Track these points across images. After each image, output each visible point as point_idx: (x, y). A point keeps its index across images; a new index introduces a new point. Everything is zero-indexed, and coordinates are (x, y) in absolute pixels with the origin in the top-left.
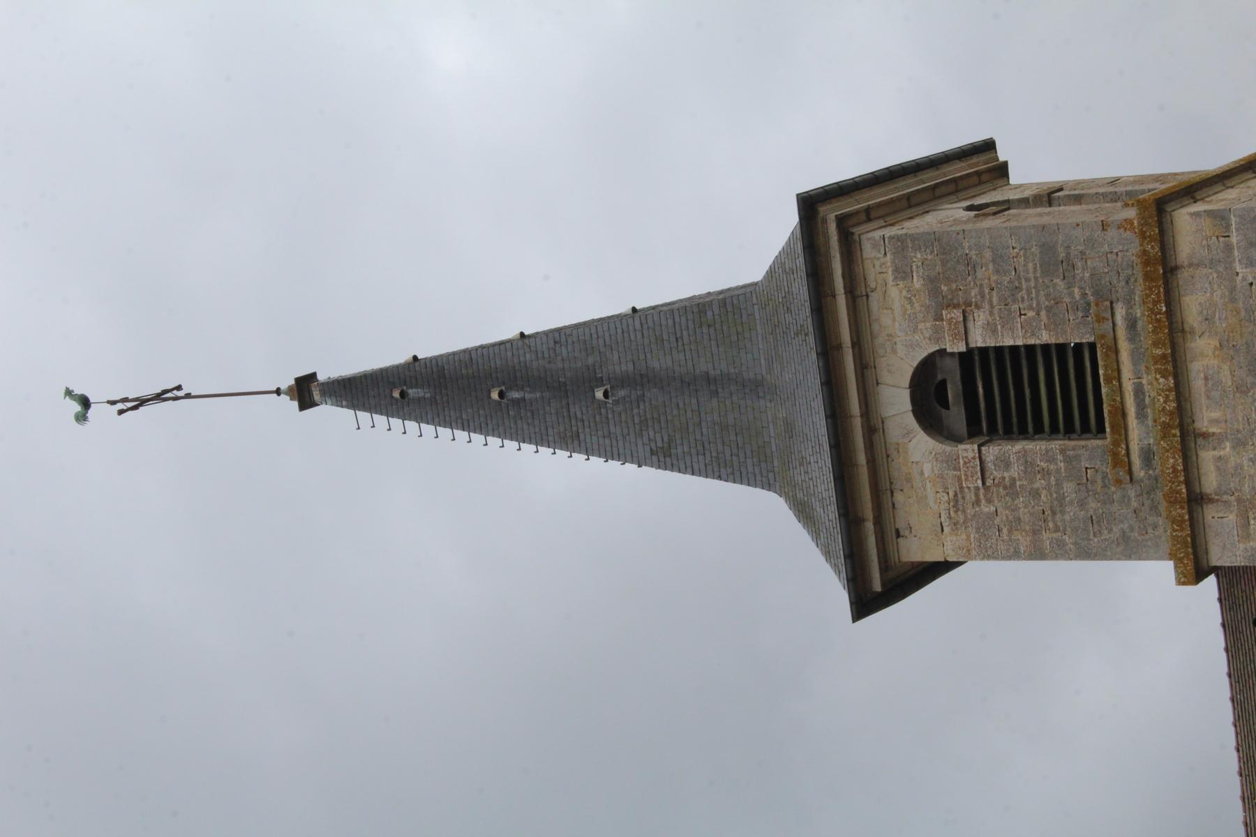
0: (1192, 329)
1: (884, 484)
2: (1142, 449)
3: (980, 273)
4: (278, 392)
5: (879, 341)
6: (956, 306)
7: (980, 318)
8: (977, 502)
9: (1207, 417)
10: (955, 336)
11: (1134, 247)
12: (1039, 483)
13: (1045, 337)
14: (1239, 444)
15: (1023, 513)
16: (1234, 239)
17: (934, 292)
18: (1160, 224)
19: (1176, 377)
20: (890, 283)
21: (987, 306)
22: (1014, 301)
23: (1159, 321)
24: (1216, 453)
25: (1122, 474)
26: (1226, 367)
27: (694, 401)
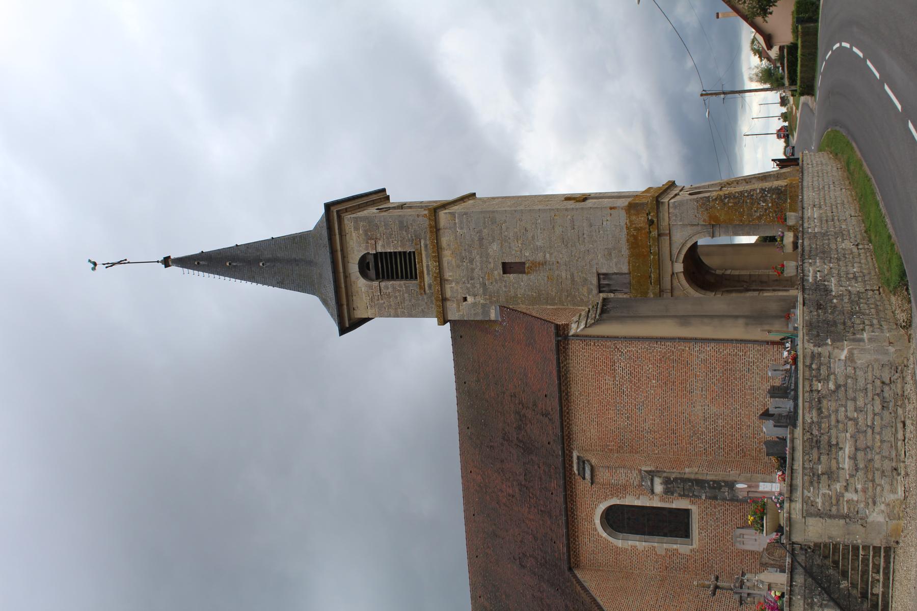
3: (380, 229)
4: (158, 262)
5: (349, 249)
6: (372, 239)
7: (380, 243)
8: (378, 300)
9: (448, 275)
10: (372, 249)
11: (427, 223)
12: (397, 294)
13: (400, 249)
14: (457, 283)
15: (392, 303)
16: (457, 221)
17: (366, 234)
18: (435, 215)
19: (439, 262)
21: (382, 239)
22: (391, 238)
23: (434, 245)
24: (450, 286)
25: (422, 291)
26: (454, 260)
27: (291, 267)
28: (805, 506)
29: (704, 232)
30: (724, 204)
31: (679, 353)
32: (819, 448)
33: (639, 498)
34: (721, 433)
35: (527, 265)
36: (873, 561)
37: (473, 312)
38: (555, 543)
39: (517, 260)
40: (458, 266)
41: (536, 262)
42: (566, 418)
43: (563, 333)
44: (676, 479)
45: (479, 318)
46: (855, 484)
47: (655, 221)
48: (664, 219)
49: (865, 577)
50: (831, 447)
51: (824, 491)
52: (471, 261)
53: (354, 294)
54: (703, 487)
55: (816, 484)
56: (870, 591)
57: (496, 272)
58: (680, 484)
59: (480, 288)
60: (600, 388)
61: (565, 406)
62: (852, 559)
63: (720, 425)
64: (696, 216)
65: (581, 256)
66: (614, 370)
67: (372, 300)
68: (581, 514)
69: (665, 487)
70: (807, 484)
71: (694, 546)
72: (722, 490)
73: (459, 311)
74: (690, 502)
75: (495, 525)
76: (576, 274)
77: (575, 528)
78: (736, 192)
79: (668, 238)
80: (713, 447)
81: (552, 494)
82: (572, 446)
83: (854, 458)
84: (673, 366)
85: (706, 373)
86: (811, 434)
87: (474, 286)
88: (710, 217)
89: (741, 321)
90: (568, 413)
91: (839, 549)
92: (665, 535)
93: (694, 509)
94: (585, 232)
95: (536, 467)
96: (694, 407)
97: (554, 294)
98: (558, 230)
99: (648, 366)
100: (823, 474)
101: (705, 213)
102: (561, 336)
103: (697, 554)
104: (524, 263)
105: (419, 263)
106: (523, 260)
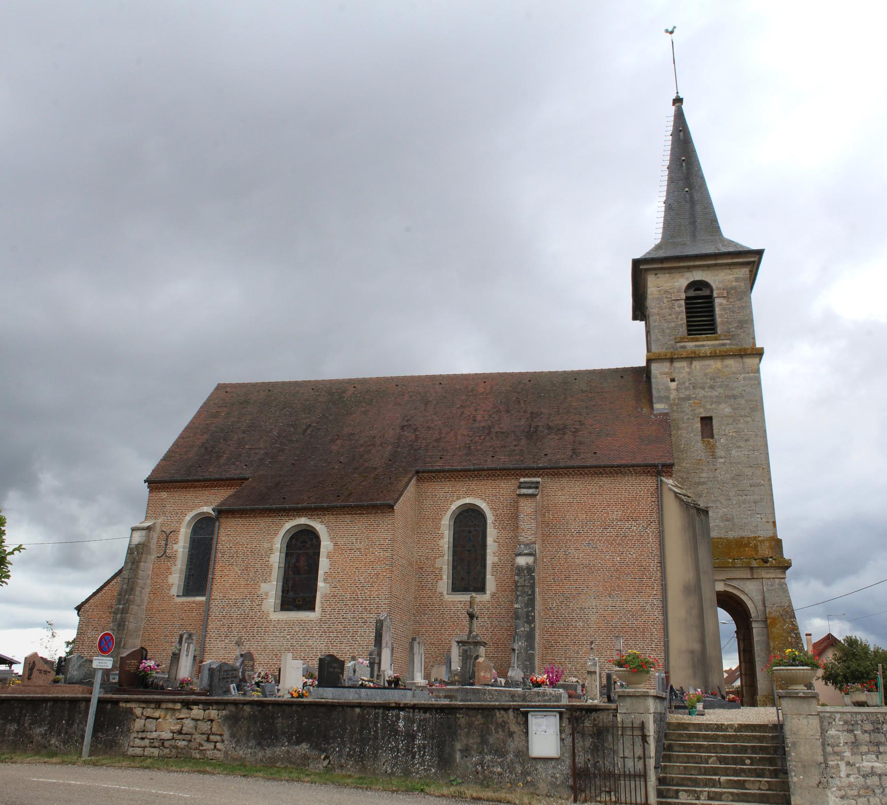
1: (673, 271)
5: (716, 272)
7: (724, 301)
8: (667, 298)
9: (697, 364)
10: (718, 294)
11: (747, 347)
12: (674, 316)
13: (718, 320)
14: (689, 373)
15: (664, 311)
16: (751, 375)
18: (756, 354)
20: (734, 276)
22: (730, 312)
25: (678, 340)
26: (711, 371)
28: (828, 715)
29: (757, 612)
30: (789, 633)
31: (650, 584)
32: (873, 731)
33: (495, 541)
35: (711, 441)
36: (725, 793)
37: (661, 387)
39: (715, 431)
40: (706, 375)
43: (664, 471)
44: (533, 578)
45: (655, 393)
46: (854, 774)
47: (766, 565)
48: (768, 573)
49: (689, 783)
50: (877, 745)
51: (841, 737)
52: (712, 387)
54: (527, 605)
55: (846, 727)
56: (681, 788)
57: (702, 410)
58: (528, 582)
59: (686, 395)
60: (608, 506)
61: (589, 471)
62: (700, 767)
64: (774, 604)
66: (628, 520)
67: (666, 292)
68: (474, 485)
69: (524, 567)
70: (845, 717)
71: (446, 596)
72: (526, 624)
73: (661, 374)
74: (494, 593)
76: (705, 486)
77: (459, 479)
78: (802, 644)
79: (749, 577)
81: (493, 457)
83: (873, 773)
86: (883, 723)
87: (687, 389)
88: (774, 619)
89: (697, 646)
91: (690, 752)
92: (454, 568)
93: (486, 597)
94: (748, 497)
95: (515, 443)
97: (684, 465)
98: (748, 471)
100: (855, 736)
103: (438, 599)
104: (712, 437)
105: (707, 337)
106: (715, 437)
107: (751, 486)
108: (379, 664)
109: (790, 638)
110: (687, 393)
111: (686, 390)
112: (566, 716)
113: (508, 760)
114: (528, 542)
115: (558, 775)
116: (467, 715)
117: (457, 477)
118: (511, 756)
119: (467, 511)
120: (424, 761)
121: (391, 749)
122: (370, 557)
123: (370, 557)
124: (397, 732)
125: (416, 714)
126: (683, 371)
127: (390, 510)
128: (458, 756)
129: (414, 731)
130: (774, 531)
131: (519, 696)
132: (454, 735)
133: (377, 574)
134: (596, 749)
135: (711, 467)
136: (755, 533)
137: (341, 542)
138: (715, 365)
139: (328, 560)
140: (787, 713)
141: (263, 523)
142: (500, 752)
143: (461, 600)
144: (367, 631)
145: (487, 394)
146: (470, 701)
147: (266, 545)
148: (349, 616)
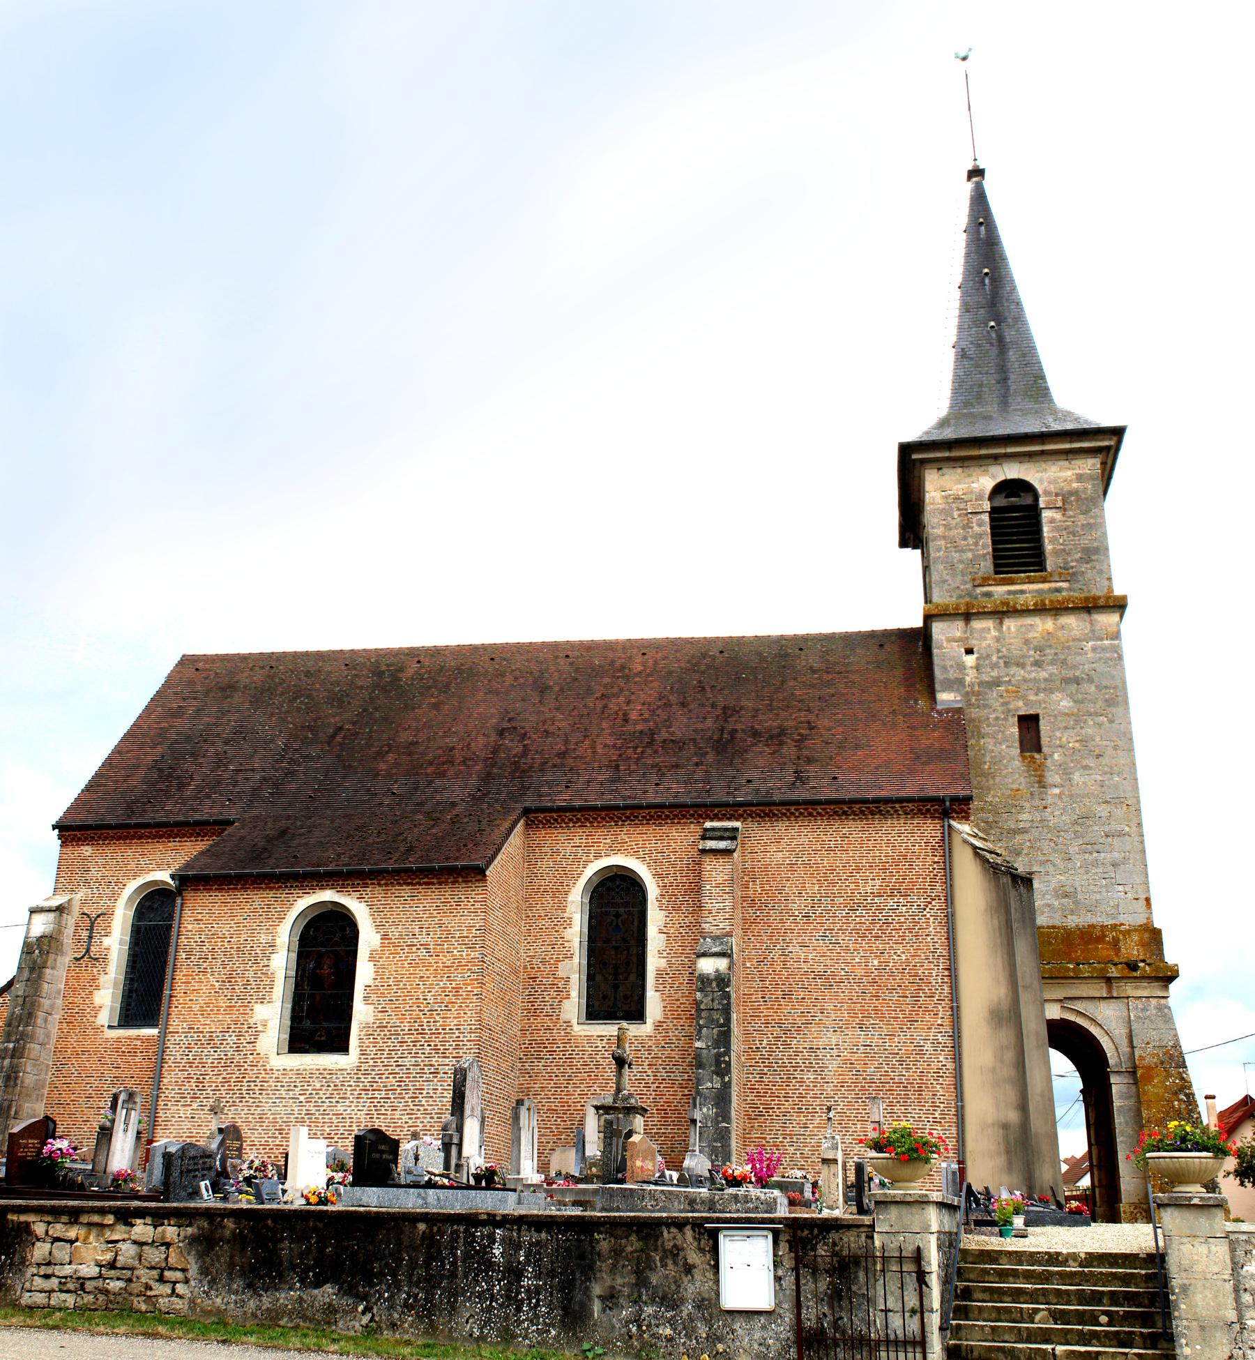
0: (1058, 619)
2: (991, 592)
3: (1081, 516)
4: (975, 160)
5: (1044, 465)
6: (1064, 504)
7: (1057, 516)
8: (959, 509)
9: (1011, 624)
10: (1048, 502)
11: (1099, 593)
13: (1048, 547)
14: (998, 640)
15: (954, 532)
16: (1106, 642)
17: (1071, 493)
18: (1114, 606)
19: (1033, 610)
20: (1074, 472)
21: (1065, 519)
22: (1068, 533)
23: (1064, 603)
24: (992, 628)
26: (1038, 635)
27: (993, 371)
28: (1244, 1237)
30: (1176, 1093)
31: (930, 1008)
34: (790, 1078)
35: (1037, 756)
37: (948, 663)
38: (567, 787)
39: (1044, 740)
40: (1026, 642)
41: (1043, 771)
42: (802, 810)
43: (954, 811)
45: (938, 674)
47: (1135, 974)
48: (1137, 988)
52: (1038, 664)
53: (965, 470)
54: (717, 1043)
57: (1021, 703)
58: (719, 1003)
59: (992, 677)
60: (858, 870)
62: (1019, 1329)
63: (805, 1077)
64: (1148, 1043)
65: (1059, 847)
67: (957, 498)
68: (625, 833)
69: (712, 977)
71: (577, 1028)
72: (715, 1077)
74: (660, 1022)
75: (562, 690)
76: (1026, 837)
77: (599, 822)
78: (1199, 1113)
79: (1105, 995)
80: (763, 1062)
81: (657, 784)
82: (750, 819)
84: (907, 997)
85: (898, 1054)
87: (994, 666)
88: (1149, 1068)
89: (1013, 1116)
90: (810, 814)
91: (1001, 1302)
92: (590, 977)
93: (647, 1029)
94: (1102, 855)
95: (695, 759)
96: (834, 1031)
97: (989, 799)
98: (1102, 810)
99: (904, 953)
101: (1155, 1060)
102: (951, 805)
104: (1039, 750)
105: (1028, 577)
106: (1045, 749)
107: (1107, 836)
108: (460, 1145)
109: (1176, 1103)
110: (995, 673)
111: (992, 668)
112: (784, 1237)
113: (684, 1314)
114: (718, 933)
115: (771, 1342)
116: (612, 1235)
117: (596, 819)
118: (688, 1308)
119: (612, 879)
120: (537, 1316)
121: (480, 1295)
122: (445, 960)
123: (445, 960)
124: (490, 1265)
125: (523, 1233)
126: (987, 635)
127: (479, 877)
128: (597, 1307)
129: (519, 1263)
130: (1147, 915)
131: (703, 1202)
132: (589, 1271)
133: (457, 989)
134: (836, 1296)
135: (1037, 802)
136: (1114, 918)
137: (394, 932)
138: (1043, 625)
139: (372, 963)
140: (1171, 1234)
141: (258, 899)
142: (670, 1301)
143: (604, 1034)
144: (440, 1088)
145: (648, 675)
146: (618, 1210)
147: (263, 938)
148: (408, 1062)
